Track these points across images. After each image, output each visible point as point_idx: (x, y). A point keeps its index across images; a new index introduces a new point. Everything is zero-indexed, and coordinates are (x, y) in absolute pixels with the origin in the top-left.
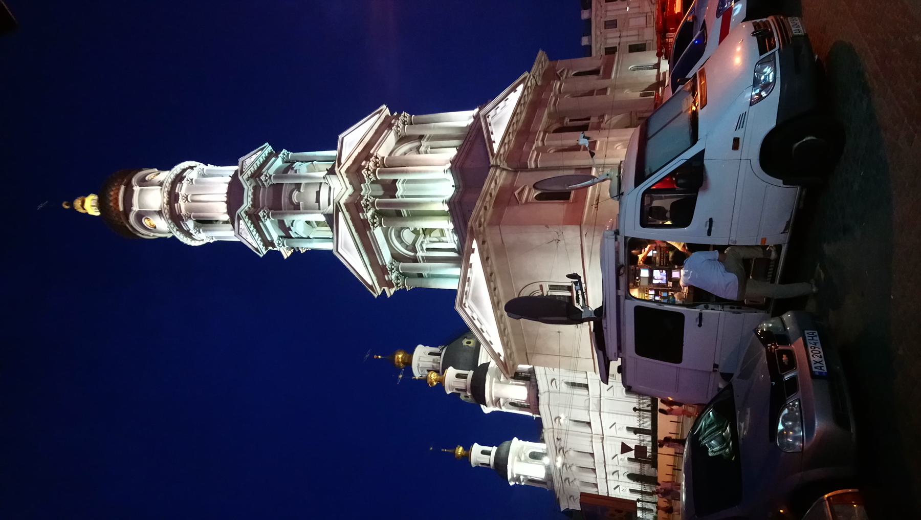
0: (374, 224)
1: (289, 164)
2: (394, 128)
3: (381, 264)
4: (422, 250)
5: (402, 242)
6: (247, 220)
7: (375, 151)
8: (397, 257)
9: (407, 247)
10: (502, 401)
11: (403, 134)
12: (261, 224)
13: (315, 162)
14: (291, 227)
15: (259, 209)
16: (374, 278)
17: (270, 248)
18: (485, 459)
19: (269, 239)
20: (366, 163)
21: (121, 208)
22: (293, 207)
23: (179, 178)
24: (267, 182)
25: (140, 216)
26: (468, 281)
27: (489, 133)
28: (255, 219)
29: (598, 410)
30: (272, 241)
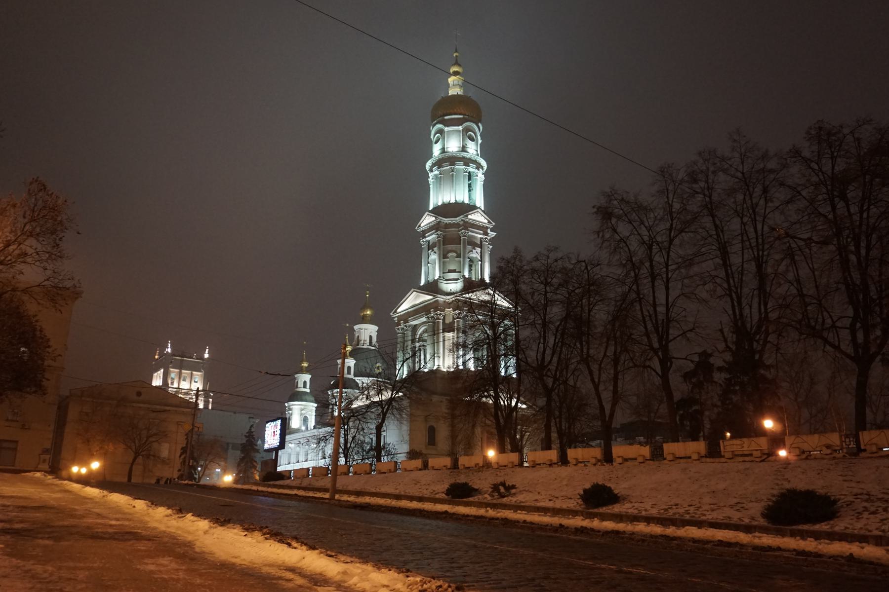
5: (424, 332)
8: (415, 328)
12: (434, 231)
13: (480, 263)
16: (401, 313)
18: (301, 384)
19: (426, 235)
21: (446, 118)
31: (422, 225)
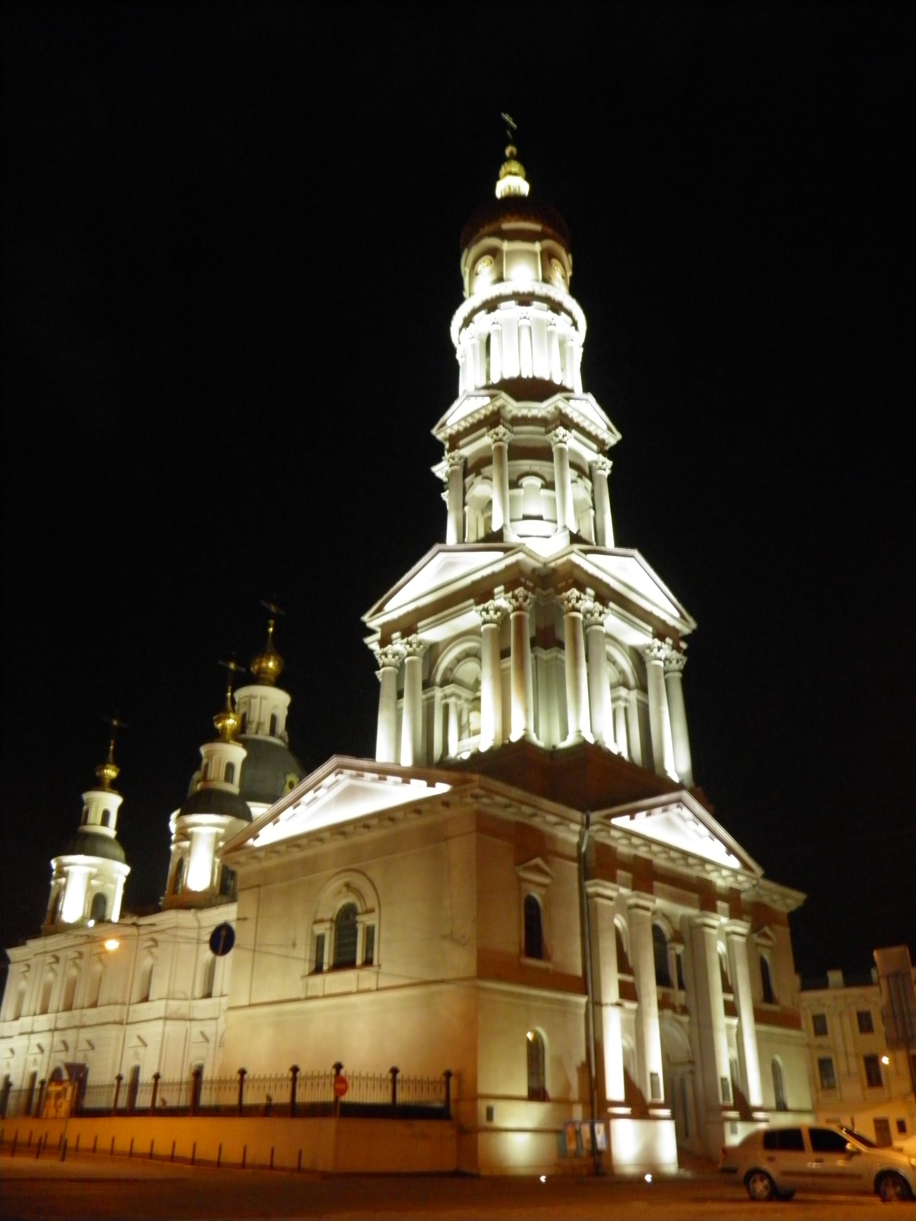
0: (487, 611)
1: (584, 472)
2: (657, 642)
3: (420, 624)
4: (446, 697)
5: (458, 660)
6: (490, 408)
7: (612, 609)
8: (432, 652)
9: (450, 669)
10: (186, 844)
11: (646, 659)
12: (484, 430)
13: (592, 512)
14: (480, 478)
15: (509, 426)
17: (447, 445)
18: (95, 816)
19: (461, 443)
20: (590, 595)
21: (507, 226)
22: (515, 478)
23: (556, 307)
24: (554, 438)
25: (494, 253)
26: (380, 779)
27: (649, 809)
28: (493, 420)
29: (168, 1015)
30: (459, 448)
31: (449, 423)
